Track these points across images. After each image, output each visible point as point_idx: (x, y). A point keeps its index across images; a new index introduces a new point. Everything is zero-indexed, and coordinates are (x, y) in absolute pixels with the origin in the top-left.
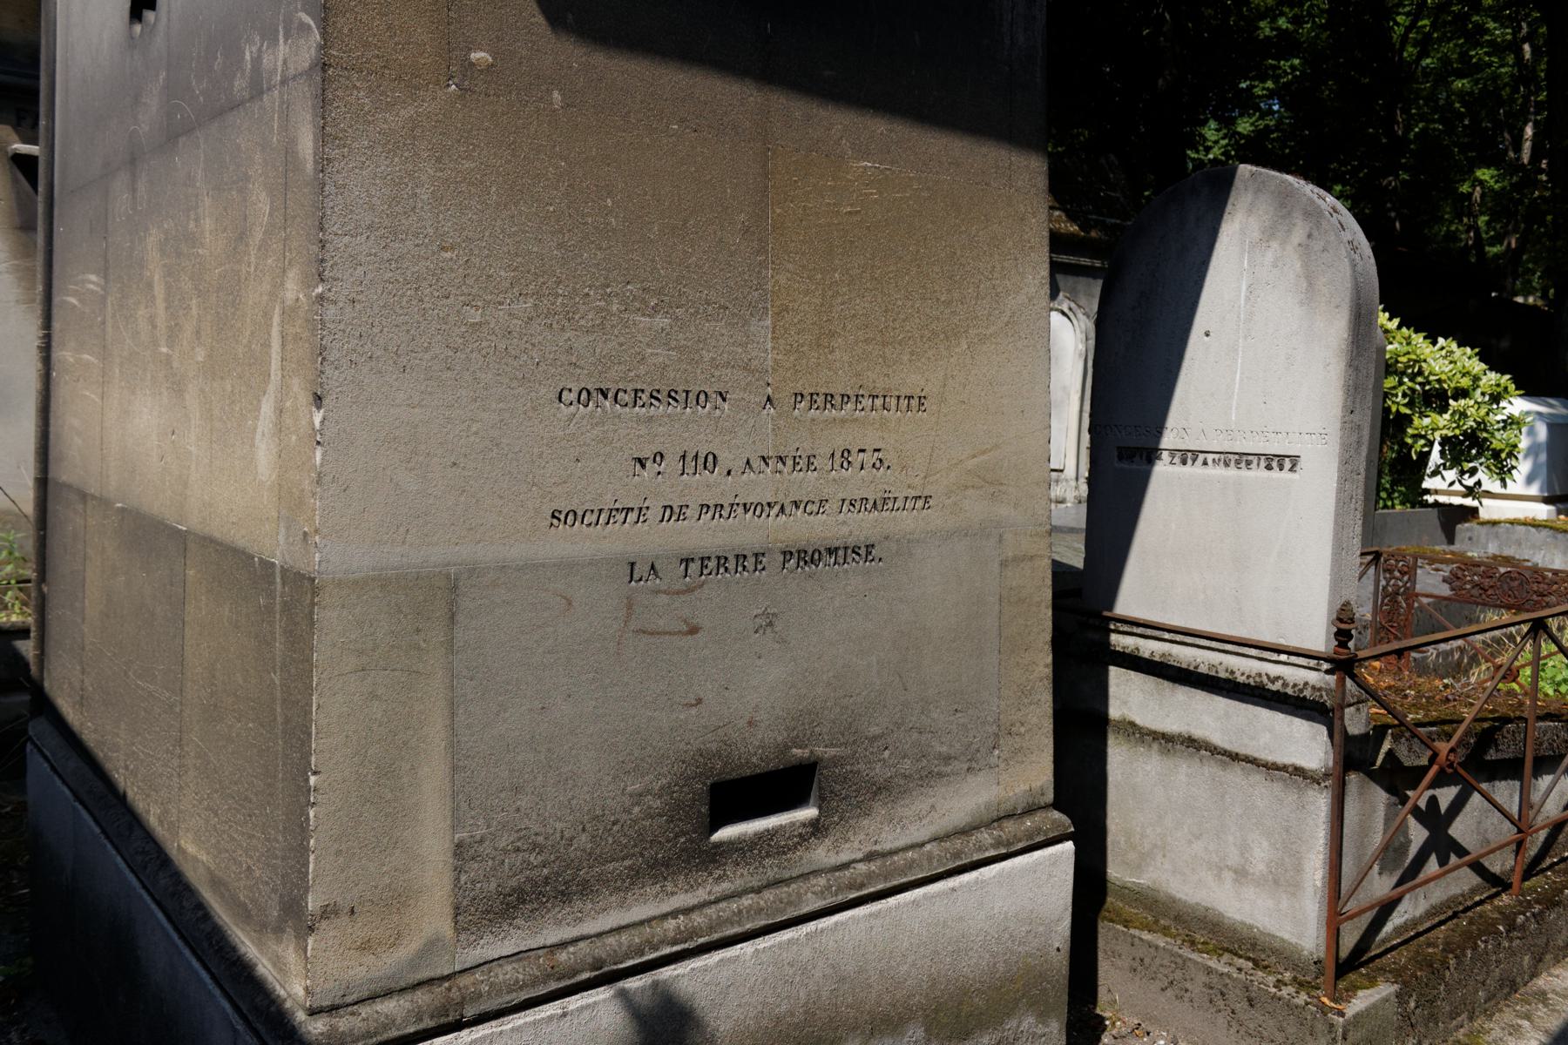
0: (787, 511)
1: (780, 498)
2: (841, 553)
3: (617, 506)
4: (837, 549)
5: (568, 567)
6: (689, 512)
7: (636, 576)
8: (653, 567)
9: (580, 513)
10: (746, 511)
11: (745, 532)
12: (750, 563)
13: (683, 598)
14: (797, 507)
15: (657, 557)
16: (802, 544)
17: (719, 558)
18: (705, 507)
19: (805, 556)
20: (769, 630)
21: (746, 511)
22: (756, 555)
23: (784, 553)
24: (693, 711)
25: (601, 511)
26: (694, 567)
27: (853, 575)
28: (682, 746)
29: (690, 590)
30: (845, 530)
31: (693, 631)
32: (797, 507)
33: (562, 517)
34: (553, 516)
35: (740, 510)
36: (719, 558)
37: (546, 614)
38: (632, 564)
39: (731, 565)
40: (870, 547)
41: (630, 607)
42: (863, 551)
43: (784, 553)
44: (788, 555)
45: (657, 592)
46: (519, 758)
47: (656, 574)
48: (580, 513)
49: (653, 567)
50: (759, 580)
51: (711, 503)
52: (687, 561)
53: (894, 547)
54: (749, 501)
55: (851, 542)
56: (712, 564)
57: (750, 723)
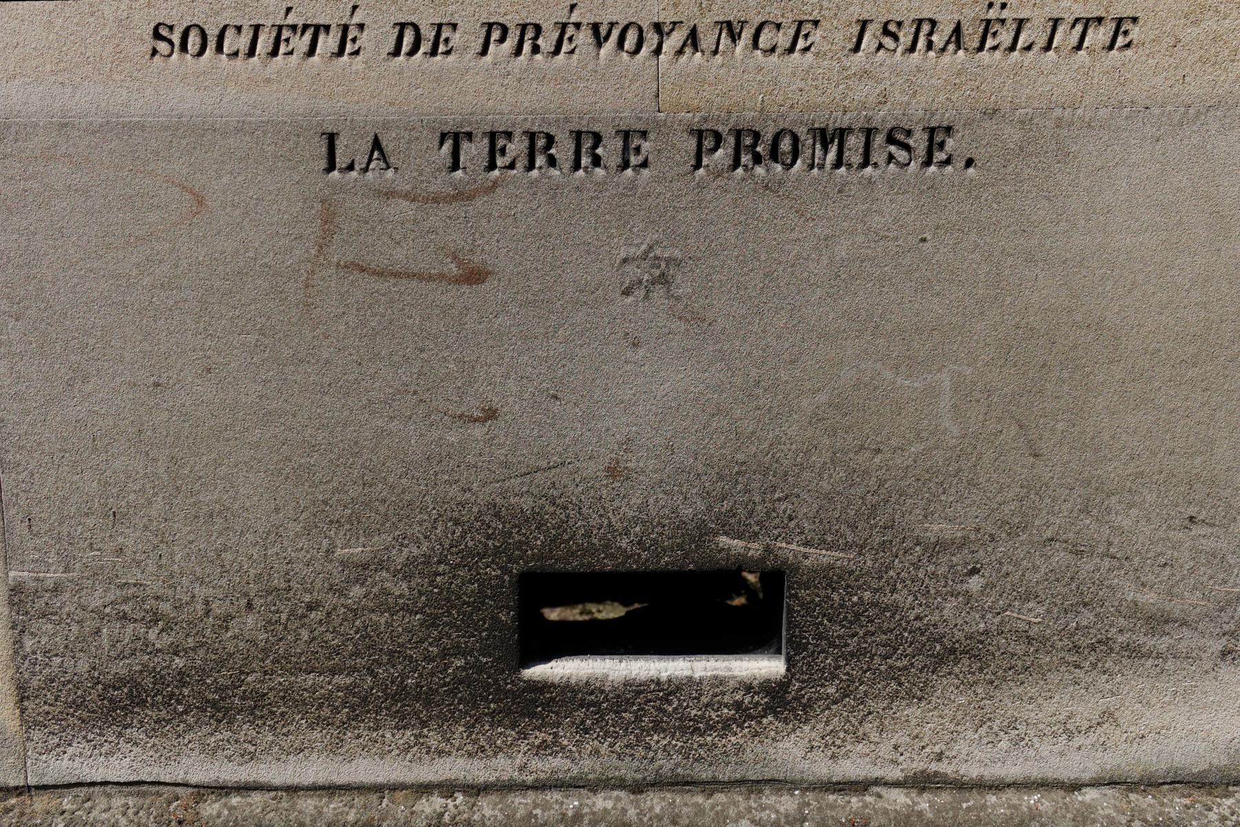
0: (707, 41)
1: (688, 12)
2: (854, 142)
3: (291, 20)
4: (842, 133)
5: (192, 133)
6: (456, 39)
7: (341, 161)
8: (377, 144)
9: (212, 33)
10: (599, 41)
11: (599, 86)
12: (610, 150)
13: (447, 210)
14: (734, 37)
15: (386, 126)
16: (749, 117)
17: (532, 136)
18: (494, 31)
19: (757, 145)
20: (658, 292)
21: (599, 41)
22: (626, 135)
23: (700, 135)
24: (478, 431)
25: (257, 28)
26: (474, 152)
27: (889, 195)
28: (454, 491)
29: (462, 196)
30: (865, 92)
31: (475, 276)
32: (734, 37)
33: (176, 38)
34: (157, 36)
35: (584, 38)
36: (532, 136)
37: (153, 217)
38: (332, 138)
39: (563, 150)
40: (937, 135)
41: (329, 218)
42: (919, 141)
43: (700, 135)
44: (705, 138)
45: (390, 194)
46: (117, 464)
47: (383, 157)
48: (212, 33)
49: (377, 144)
50: (632, 185)
51: (511, 20)
52: (456, 138)
53: (1013, 135)
54: (605, 18)
55: (883, 117)
56: (517, 147)
57: (613, 472)
